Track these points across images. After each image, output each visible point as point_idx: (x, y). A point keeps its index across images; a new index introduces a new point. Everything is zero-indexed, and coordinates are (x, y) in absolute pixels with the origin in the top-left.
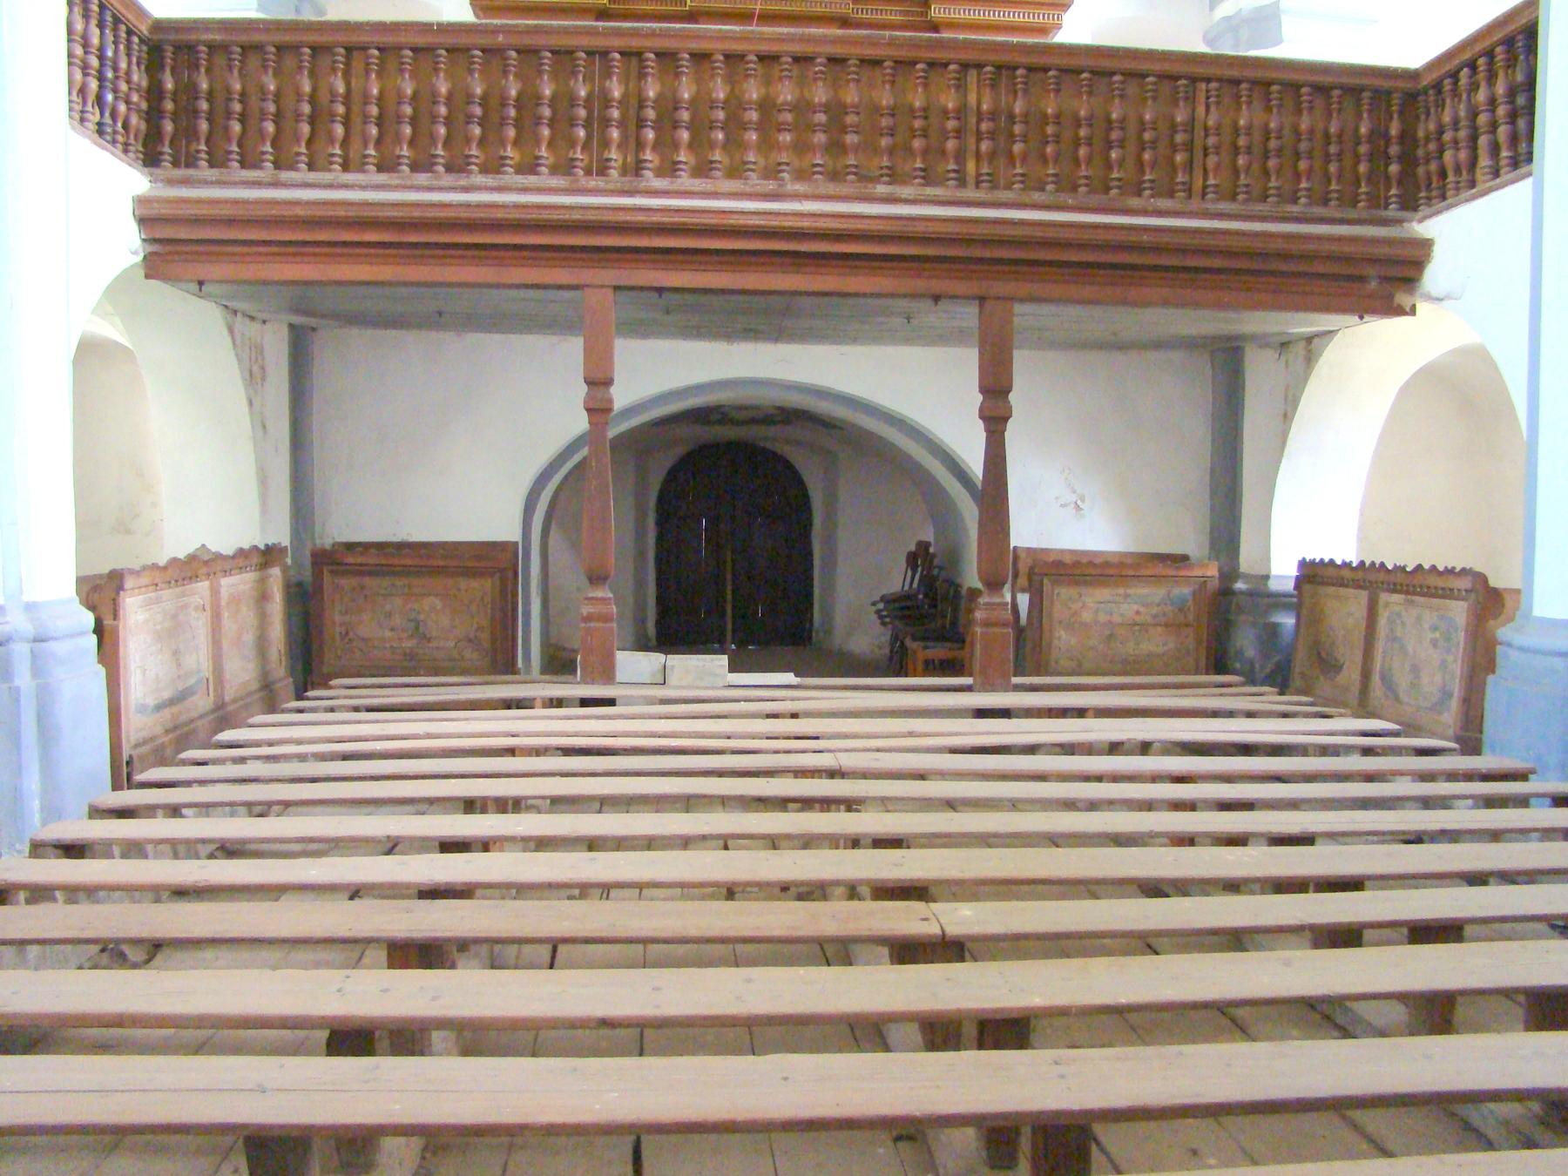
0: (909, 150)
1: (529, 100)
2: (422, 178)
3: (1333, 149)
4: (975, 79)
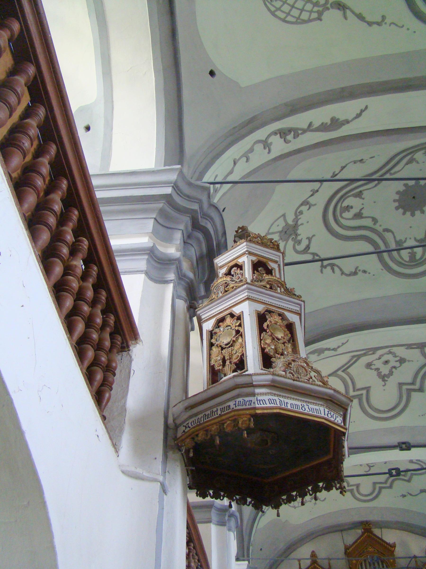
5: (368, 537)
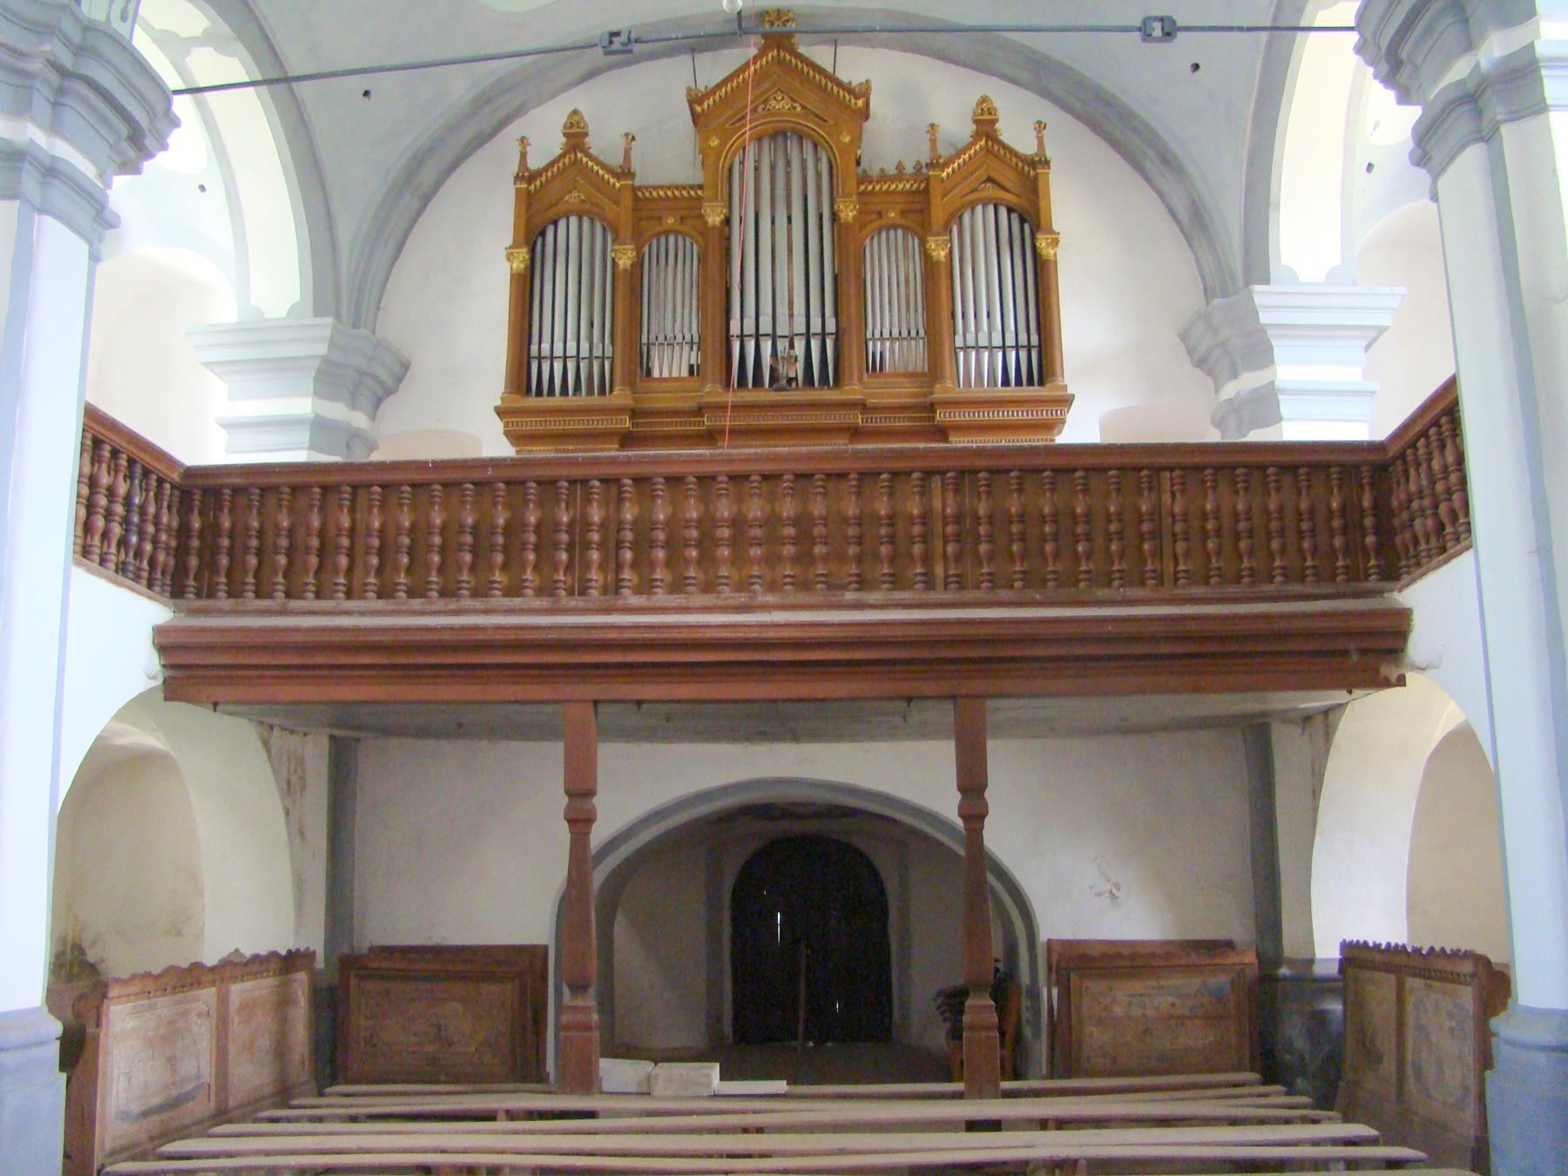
0: (877, 558)
2: (417, 603)
5: (780, 62)
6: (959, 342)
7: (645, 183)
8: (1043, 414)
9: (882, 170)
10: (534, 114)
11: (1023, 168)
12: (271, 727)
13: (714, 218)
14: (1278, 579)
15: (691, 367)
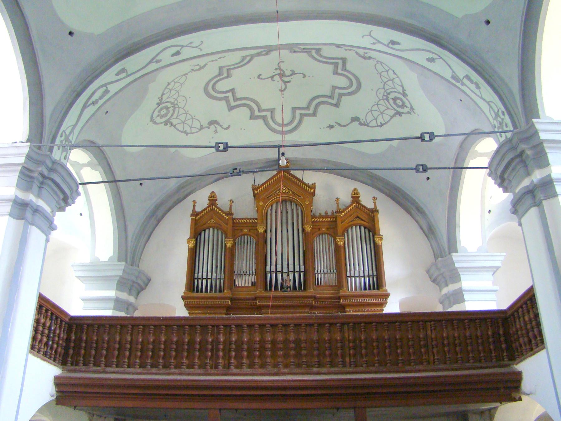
0: (325, 355)
1: (191, 343)
2: (154, 370)
3: (480, 341)
4: (347, 328)
6: (348, 274)
7: (238, 217)
8: (379, 300)
9: (320, 214)
10: (198, 192)
11: (369, 213)
12: (93, 415)
13: (261, 230)
14: (471, 361)
15: (252, 283)
